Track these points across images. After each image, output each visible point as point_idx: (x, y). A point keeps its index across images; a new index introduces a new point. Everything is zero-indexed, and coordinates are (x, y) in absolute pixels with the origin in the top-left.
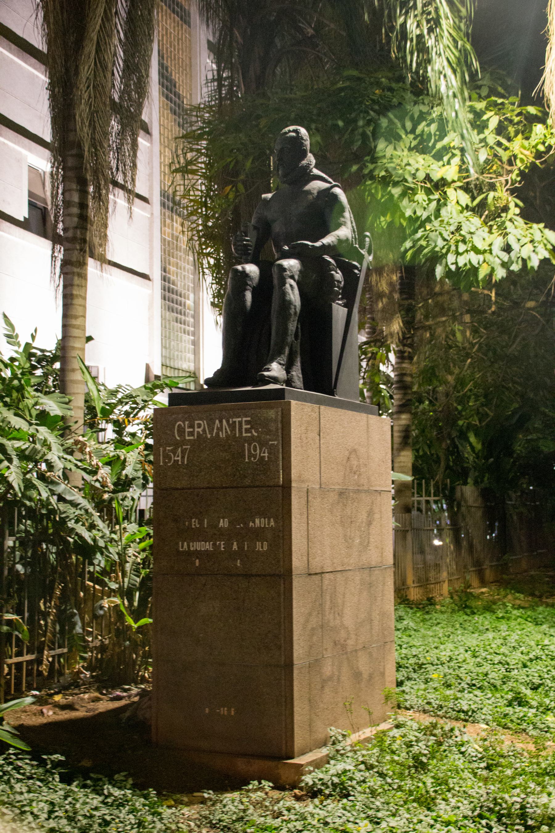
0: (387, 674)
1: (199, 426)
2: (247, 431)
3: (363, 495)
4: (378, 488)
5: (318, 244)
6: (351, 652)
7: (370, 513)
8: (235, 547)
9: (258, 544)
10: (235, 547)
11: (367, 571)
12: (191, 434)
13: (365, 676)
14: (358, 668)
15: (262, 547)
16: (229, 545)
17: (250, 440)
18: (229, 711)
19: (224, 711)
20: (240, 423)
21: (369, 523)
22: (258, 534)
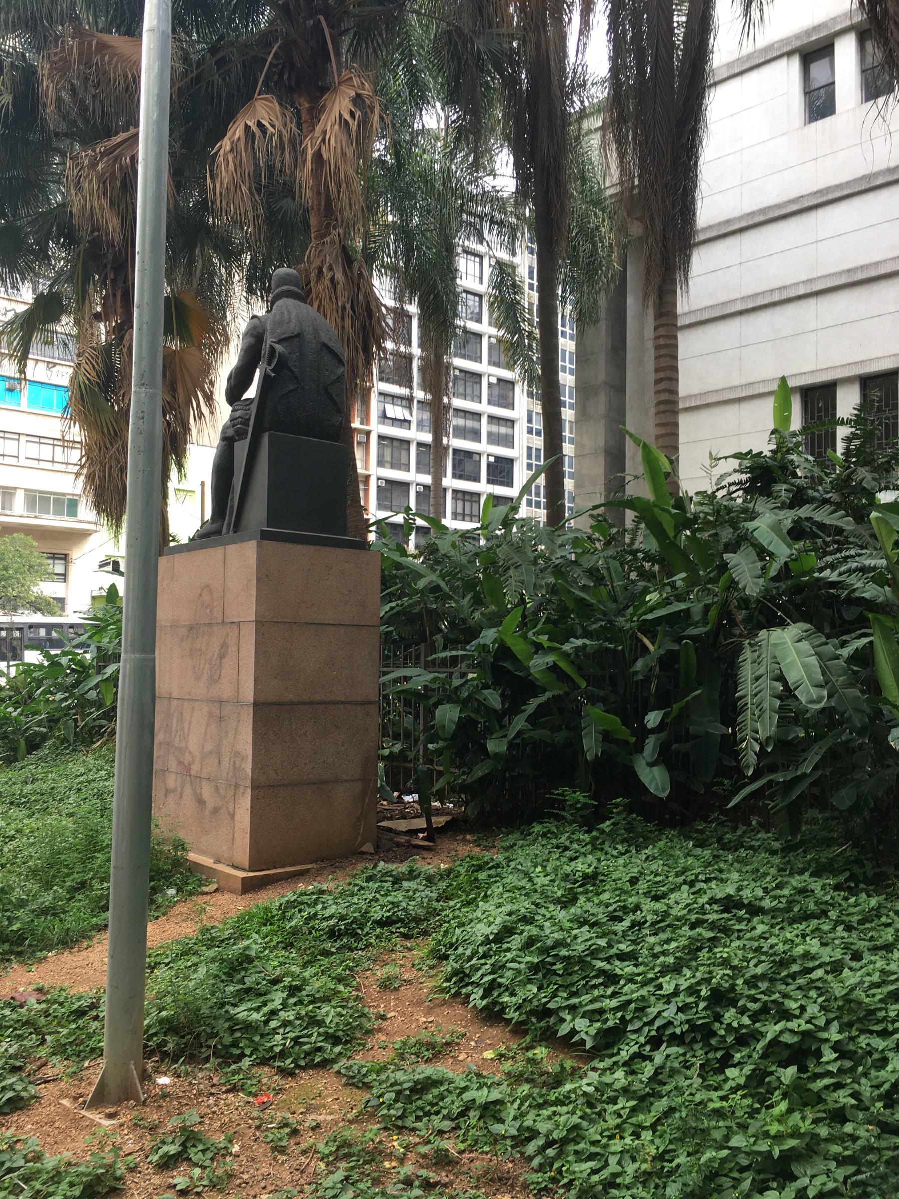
4: (235, 620)
7: (224, 646)
11: (217, 705)
21: (222, 657)
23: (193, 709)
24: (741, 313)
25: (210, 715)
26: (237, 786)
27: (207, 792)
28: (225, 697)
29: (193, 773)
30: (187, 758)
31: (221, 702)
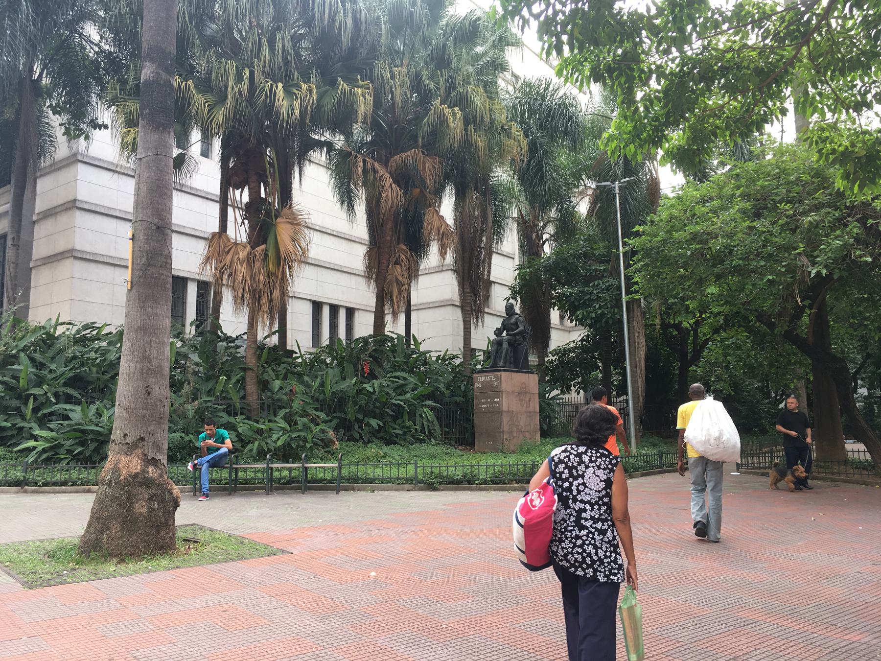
22: (496, 402)
24: (117, 217)
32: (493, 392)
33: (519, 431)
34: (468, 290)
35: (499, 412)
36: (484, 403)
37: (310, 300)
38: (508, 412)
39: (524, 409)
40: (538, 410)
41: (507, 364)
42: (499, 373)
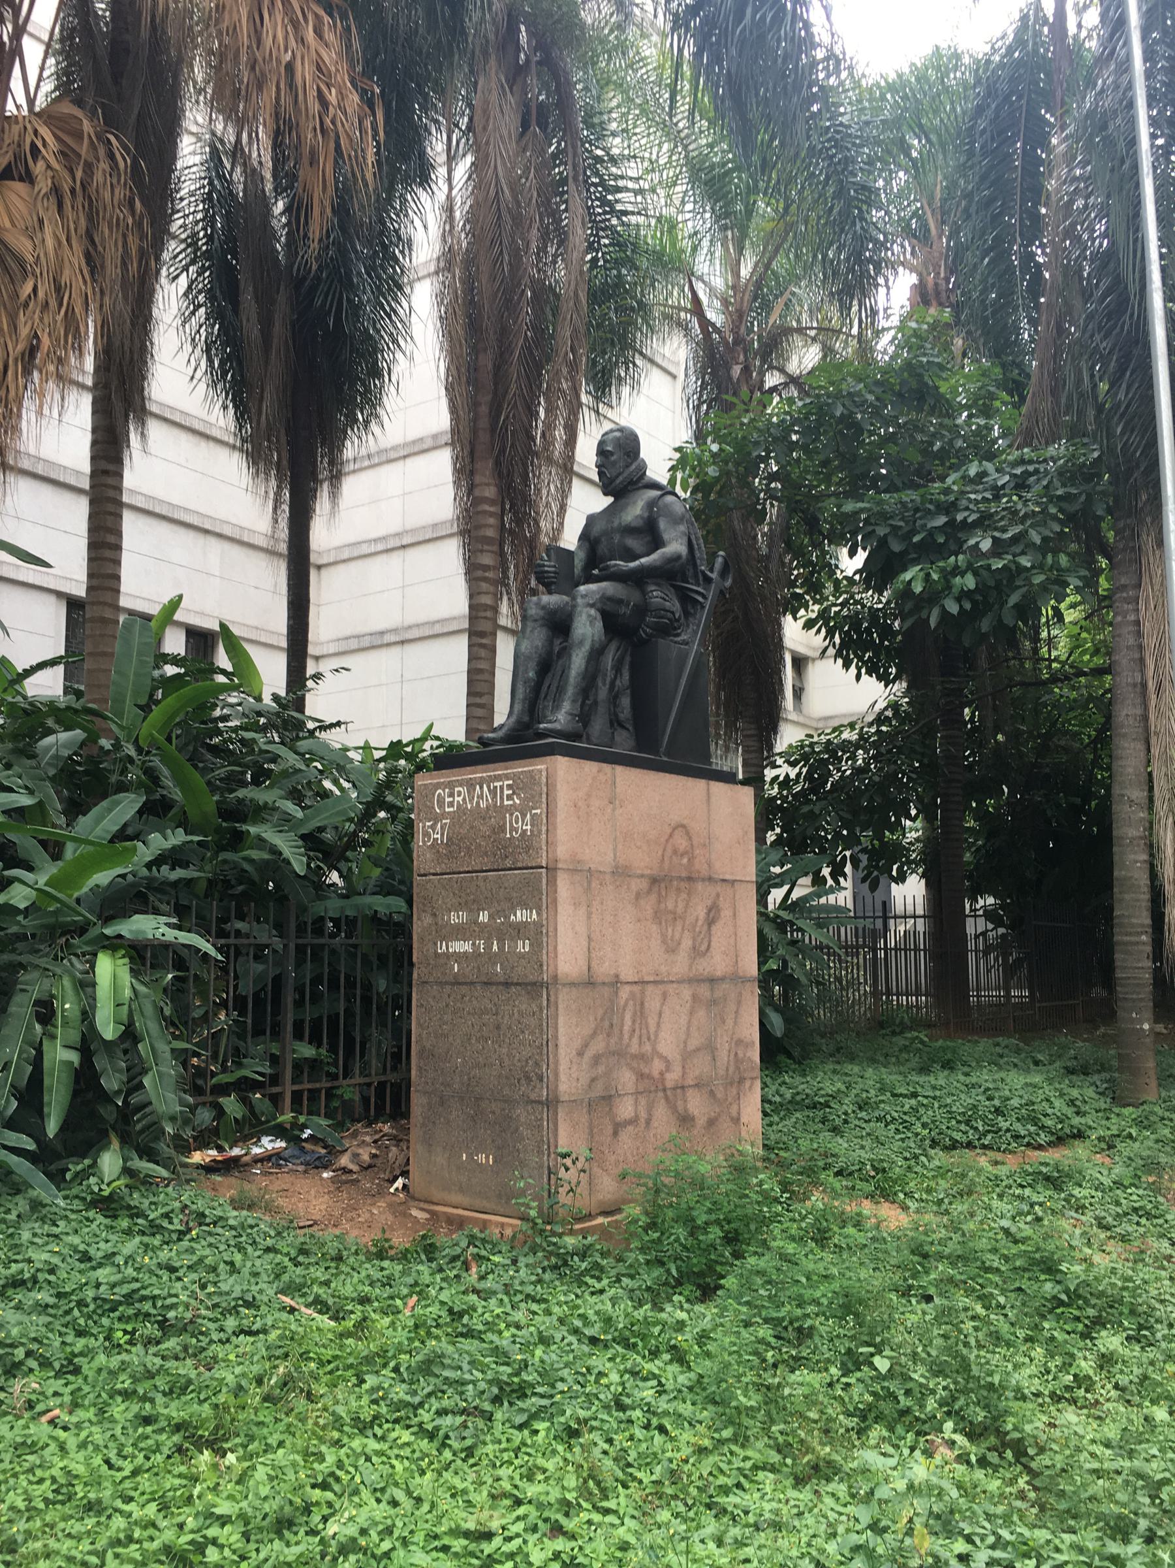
0: (744, 1119)
1: (459, 794)
2: (509, 797)
3: (700, 886)
4: (727, 877)
5: (632, 565)
6: (675, 1089)
8: (495, 948)
9: (520, 943)
10: (495, 948)
12: (451, 804)
13: (701, 1121)
14: (686, 1110)
15: (523, 947)
16: (489, 946)
17: (511, 809)
18: (487, 1158)
19: (482, 1158)
20: (502, 788)
21: (711, 922)
22: (520, 930)
23: (665, 996)
25: (695, 998)
26: (742, 1080)
27: (696, 1104)
28: (719, 974)
29: (669, 1084)
30: (657, 1066)
31: (712, 981)
32: (511, 869)
33: (652, 1087)
34: (490, 492)
35: (536, 986)
36: (459, 932)
37: (59, 594)
38: (590, 983)
39: (680, 965)
40: (750, 964)
41: (598, 725)
42: (539, 766)
